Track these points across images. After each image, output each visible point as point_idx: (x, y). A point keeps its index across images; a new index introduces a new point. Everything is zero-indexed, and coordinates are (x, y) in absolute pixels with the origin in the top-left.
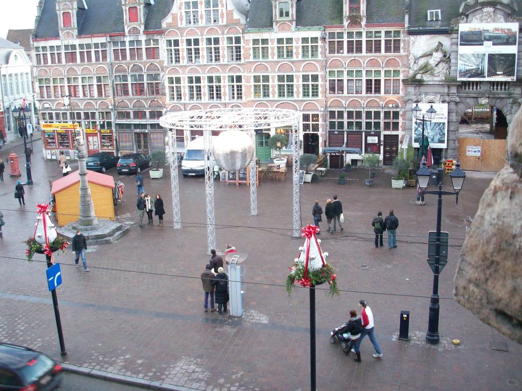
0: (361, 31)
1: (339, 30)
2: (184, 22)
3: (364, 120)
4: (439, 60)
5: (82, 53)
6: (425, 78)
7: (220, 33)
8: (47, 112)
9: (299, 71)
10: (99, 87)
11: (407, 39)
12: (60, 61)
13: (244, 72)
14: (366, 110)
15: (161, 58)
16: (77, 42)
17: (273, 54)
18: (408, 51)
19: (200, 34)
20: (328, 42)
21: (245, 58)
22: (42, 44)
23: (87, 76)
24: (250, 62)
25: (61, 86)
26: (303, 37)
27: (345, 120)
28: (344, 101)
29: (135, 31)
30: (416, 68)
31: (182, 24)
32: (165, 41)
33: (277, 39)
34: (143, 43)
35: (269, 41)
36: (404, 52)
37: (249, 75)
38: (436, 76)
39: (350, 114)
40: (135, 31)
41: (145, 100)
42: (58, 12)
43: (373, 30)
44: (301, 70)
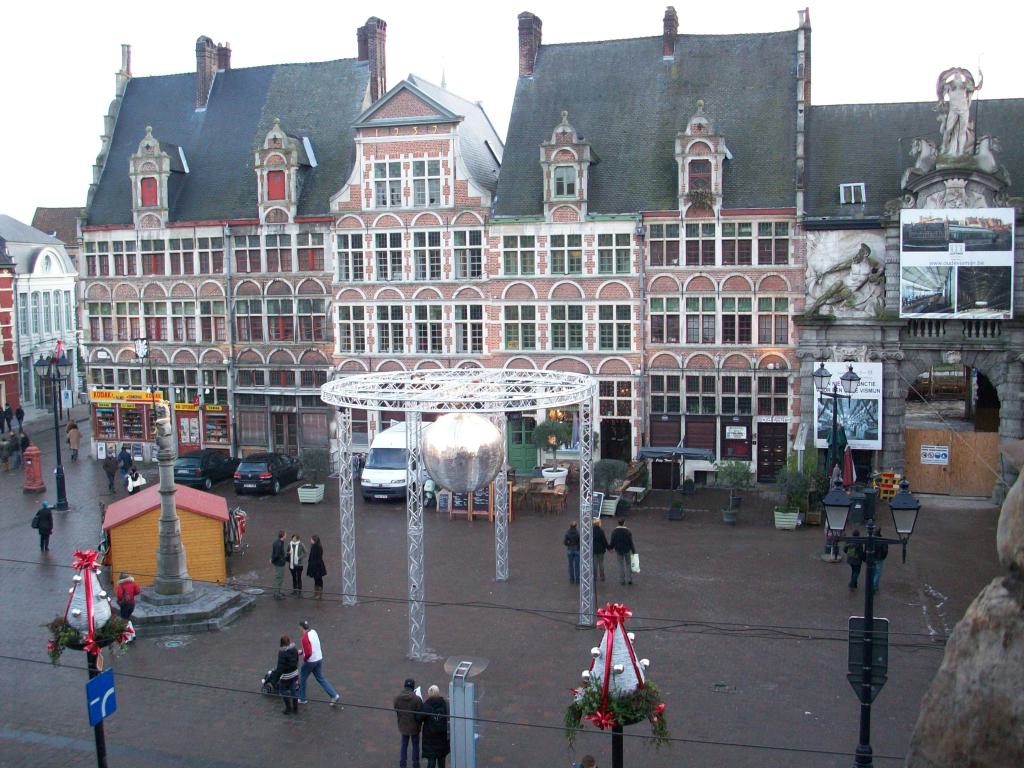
0: (713, 222)
1: (670, 221)
2: (373, 201)
3: (719, 395)
4: (863, 278)
5: (174, 257)
6: (837, 313)
7: (441, 223)
8: (102, 368)
9: (593, 299)
10: (205, 322)
11: (800, 237)
12: (131, 270)
13: (487, 298)
14: (722, 374)
15: (327, 270)
16: (166, 235)
17: (543, 266)
18: (804, 261)
20: (649, 245)
21: (489, 272)
22: (99, 237)
23: (183, 301)
24: (498, 281)
25: (131, 319)
26: (601, 233)
27: (683, 394)
28: (681, 355)
29: (278, 217)
30: (819, 293)
31: (369, 205)
32: (336, 237)
33: (552, 237)
34: (294, 239)
36: (796, 262)
37: (496, 304)
38: (858, 310)
39: (692, 383)
40: (278, 217)
41: (294, 349)
42: (133, 178)
43: (736, 220)
44: (597, 296)
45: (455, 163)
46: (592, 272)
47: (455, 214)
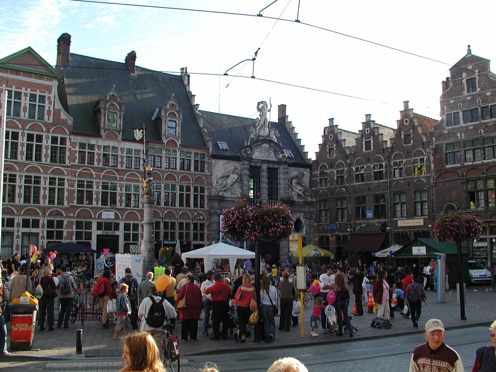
0: (176, 149)
7: (45, 130)
11: (210, 161)
13: (68, 175)
14: (179, 221)
18: (211, 172)
19: (20, 127)
35: (96, 147)
36: (208, 172)
37: (73, 179)
38: (233, 194)
45: (54, 98)
46: (123, 167)
47: (53, 126)
